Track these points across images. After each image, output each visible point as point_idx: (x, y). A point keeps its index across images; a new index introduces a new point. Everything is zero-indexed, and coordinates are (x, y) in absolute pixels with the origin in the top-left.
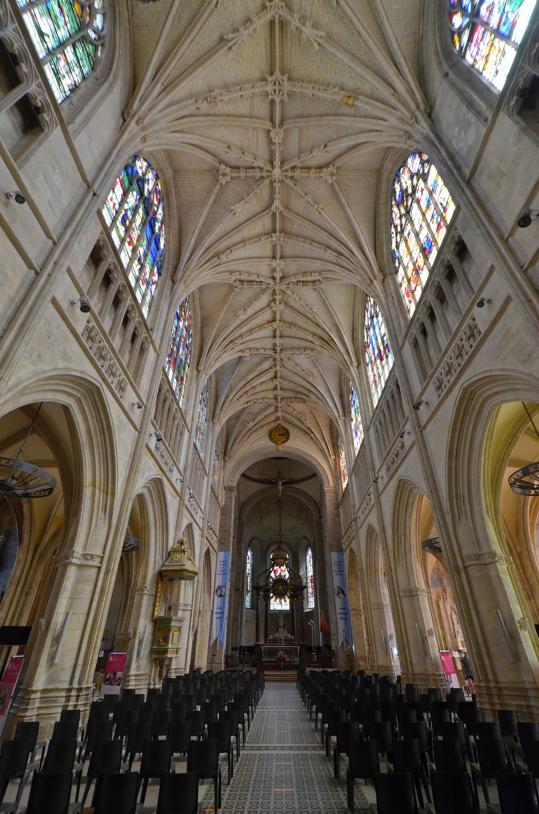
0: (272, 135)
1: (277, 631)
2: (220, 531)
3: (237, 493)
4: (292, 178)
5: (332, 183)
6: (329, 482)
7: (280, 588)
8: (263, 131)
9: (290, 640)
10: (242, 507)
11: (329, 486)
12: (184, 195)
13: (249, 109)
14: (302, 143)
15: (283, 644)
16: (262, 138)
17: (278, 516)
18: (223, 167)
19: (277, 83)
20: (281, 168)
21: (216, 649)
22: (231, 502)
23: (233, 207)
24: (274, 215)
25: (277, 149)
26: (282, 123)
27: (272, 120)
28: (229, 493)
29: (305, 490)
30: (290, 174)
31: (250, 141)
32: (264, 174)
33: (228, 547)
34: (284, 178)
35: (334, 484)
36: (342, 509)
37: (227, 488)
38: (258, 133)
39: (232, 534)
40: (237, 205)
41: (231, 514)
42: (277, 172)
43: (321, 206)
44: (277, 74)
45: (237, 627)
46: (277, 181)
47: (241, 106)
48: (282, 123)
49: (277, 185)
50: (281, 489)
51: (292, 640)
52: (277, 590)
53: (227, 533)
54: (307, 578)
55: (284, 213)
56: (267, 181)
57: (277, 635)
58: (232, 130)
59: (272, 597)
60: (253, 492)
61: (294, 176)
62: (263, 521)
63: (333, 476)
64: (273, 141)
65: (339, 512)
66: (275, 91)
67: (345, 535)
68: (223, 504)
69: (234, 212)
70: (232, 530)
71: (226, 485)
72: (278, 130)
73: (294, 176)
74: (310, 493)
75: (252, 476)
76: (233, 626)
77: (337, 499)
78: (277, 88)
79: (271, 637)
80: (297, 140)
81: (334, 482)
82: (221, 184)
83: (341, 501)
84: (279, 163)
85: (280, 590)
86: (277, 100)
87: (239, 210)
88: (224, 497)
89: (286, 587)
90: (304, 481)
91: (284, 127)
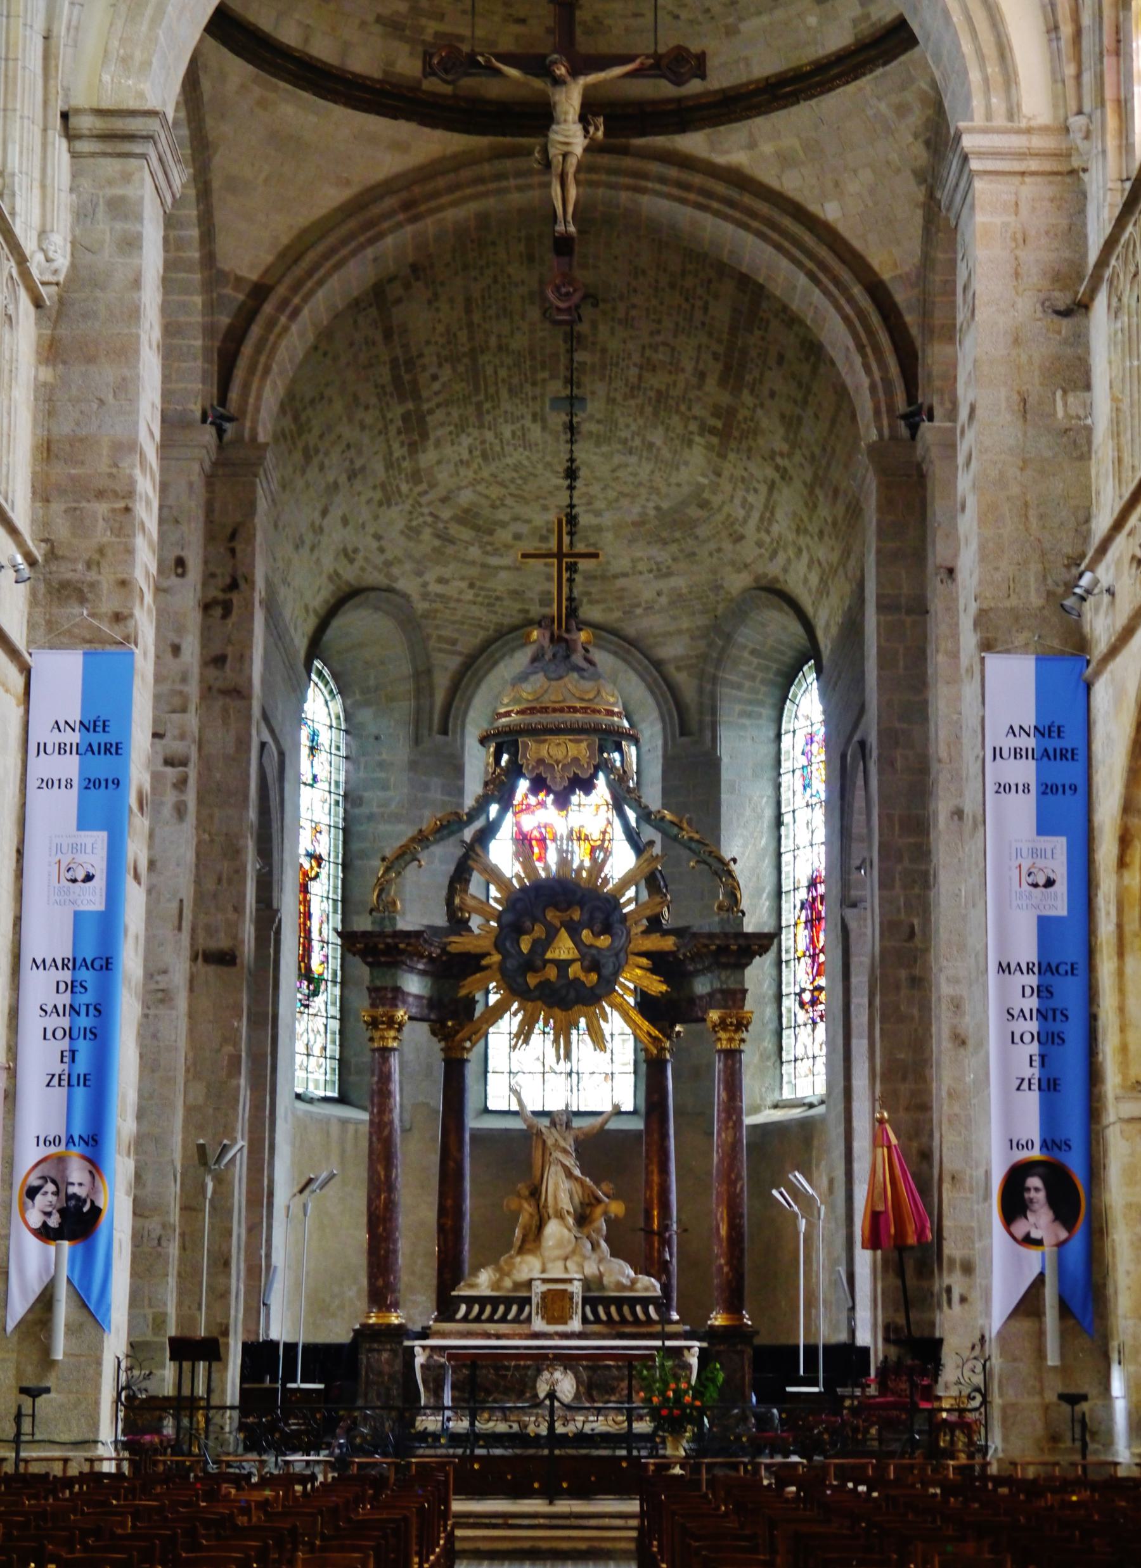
1: (533, 1238)
2: (42, 493)
3: (180, 176)
6: (1009, 79)
7: (564, 948)
9: (633, 1302)
10: (247, 316)
11: (1012, 113)
15: (575, 1325)
17: (558, 419)
21: (46, 1350)
22: (131, 244)
28: (112, 166)
29: (791, 184)
33: (118, 618)
35: (1058, 100)
36: (1115, 313)
37: (85, 123)
39: (147, 514)
41: (127, 352)
45: (222, 1210)
50: (578, 144)
51: (645, 1302)
52: (531, 963)
53: (102, 508)
54: (779, 893)
57: (528, 1267)
59: (495, 1013)
60: (332, 197)
62: (427, 458)
63: (1053, 29)
65: (1080, 339)
67: (1118, 525)
68: (63, 262)
70: (146, 487)
71: (81, 99)
74: (831, 212)
75: (323, 49)
76: (189, 1209)
77: (1075, 233)
79: (483, 1282)
81: (1056, 77)
83: (1110, 244)
85: (563, 965)
88: (63, 201)
89: (604, 941)
90: (793, 99)
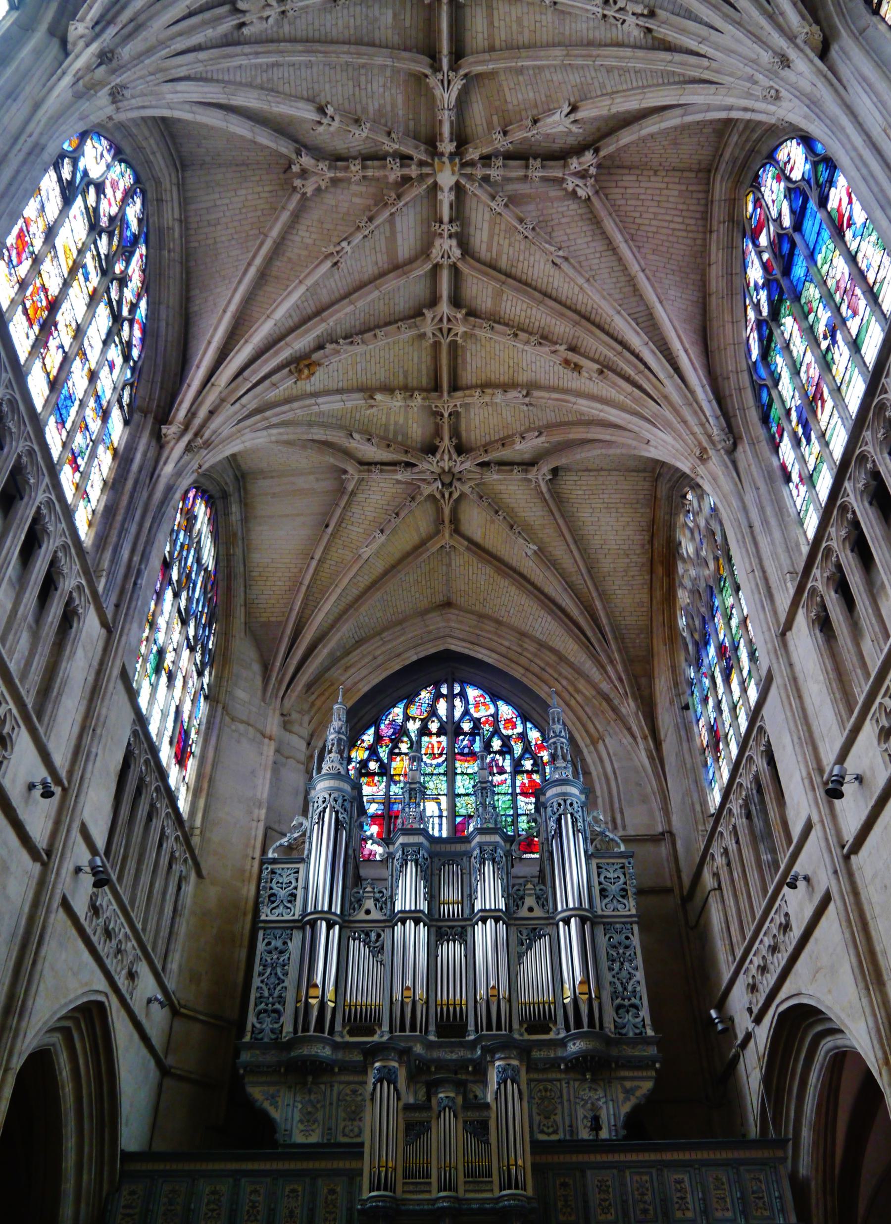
0: (457, 252)
4: (405, 159)
5: (299, 154)
8: (477, 249)
12: (704, 131)
13: (505, 298)
14: (388, 234)
16: (480, 239)
18: (581, 192)
19: (445, 331)
20: (435, 184)
23: (574, 129)
24: (458, 55)
25: (445, 227)
26: (436, 267)
27: (455, 272)
30: (413, 171)
31: (507, 241)
32: (479, 172)
34: (429, 161)
38: (489, 249)
40: (562, 128)
42: (446, 178)
43: (321, 129)
44: (444, 308)
46: (445, 159)
47: (518, 308)
48: (436, 267)
49: (447, 147)
55: (428, 71)
56: (473, 154)
58: (545, 279)
61: (402, 166)
64: (454, 242)
66: (449, 320)
69: (572, 117)
72: (445, 262)
73: (402, 166)
78: (445, 325)
80: (399, 236)
82: (597, 151)
84: (440, 196)
86: (445, 342)
87: (556, 117)
91: (428, 267)
